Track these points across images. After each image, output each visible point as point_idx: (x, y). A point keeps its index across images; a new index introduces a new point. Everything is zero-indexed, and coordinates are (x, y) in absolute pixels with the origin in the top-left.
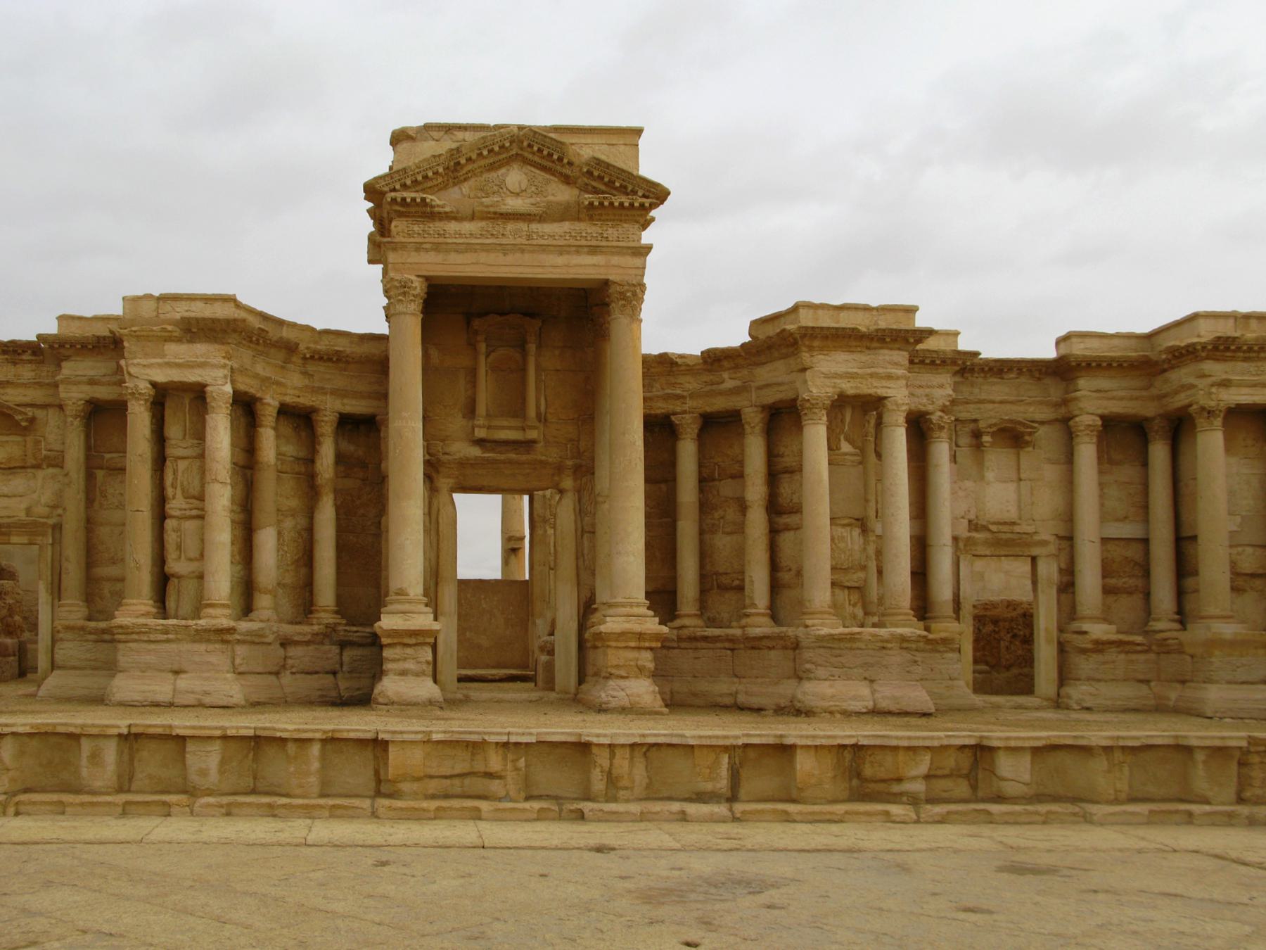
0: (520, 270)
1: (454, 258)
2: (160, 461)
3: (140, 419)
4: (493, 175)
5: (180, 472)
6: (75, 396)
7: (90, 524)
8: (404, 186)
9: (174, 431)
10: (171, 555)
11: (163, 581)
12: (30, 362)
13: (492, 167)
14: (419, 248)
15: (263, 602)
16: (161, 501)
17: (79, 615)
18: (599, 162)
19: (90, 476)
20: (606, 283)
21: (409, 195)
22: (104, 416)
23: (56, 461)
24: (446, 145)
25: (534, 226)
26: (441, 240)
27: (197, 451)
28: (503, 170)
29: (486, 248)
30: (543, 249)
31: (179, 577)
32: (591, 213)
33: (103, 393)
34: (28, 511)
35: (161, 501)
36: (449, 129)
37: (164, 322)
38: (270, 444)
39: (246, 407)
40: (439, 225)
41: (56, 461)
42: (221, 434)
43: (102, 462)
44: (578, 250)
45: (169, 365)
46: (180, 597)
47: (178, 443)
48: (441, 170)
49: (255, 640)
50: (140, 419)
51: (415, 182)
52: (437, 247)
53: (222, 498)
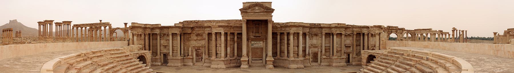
2: (216, 40)
3: (214, 36)
5: (218, 42)
6: (207, 32)
7: (209, 46)
9: (218, 37)
11: (217, 54)
15: (228, 56)
16: (216, 45)
19: (208, 41)
22: (210, 34)
23: (205, 39)
24: (249, 5)
33: (210, 32)
35: (216, 45)
38: (229, 38)
39: (226, 34)
41: (205, 39)
42: (223, 38)
43: (209, 40)
46: (219, 55)
47: (218, 39)
49: (227, 60)
50: (214, 36)
53: (223, 45)
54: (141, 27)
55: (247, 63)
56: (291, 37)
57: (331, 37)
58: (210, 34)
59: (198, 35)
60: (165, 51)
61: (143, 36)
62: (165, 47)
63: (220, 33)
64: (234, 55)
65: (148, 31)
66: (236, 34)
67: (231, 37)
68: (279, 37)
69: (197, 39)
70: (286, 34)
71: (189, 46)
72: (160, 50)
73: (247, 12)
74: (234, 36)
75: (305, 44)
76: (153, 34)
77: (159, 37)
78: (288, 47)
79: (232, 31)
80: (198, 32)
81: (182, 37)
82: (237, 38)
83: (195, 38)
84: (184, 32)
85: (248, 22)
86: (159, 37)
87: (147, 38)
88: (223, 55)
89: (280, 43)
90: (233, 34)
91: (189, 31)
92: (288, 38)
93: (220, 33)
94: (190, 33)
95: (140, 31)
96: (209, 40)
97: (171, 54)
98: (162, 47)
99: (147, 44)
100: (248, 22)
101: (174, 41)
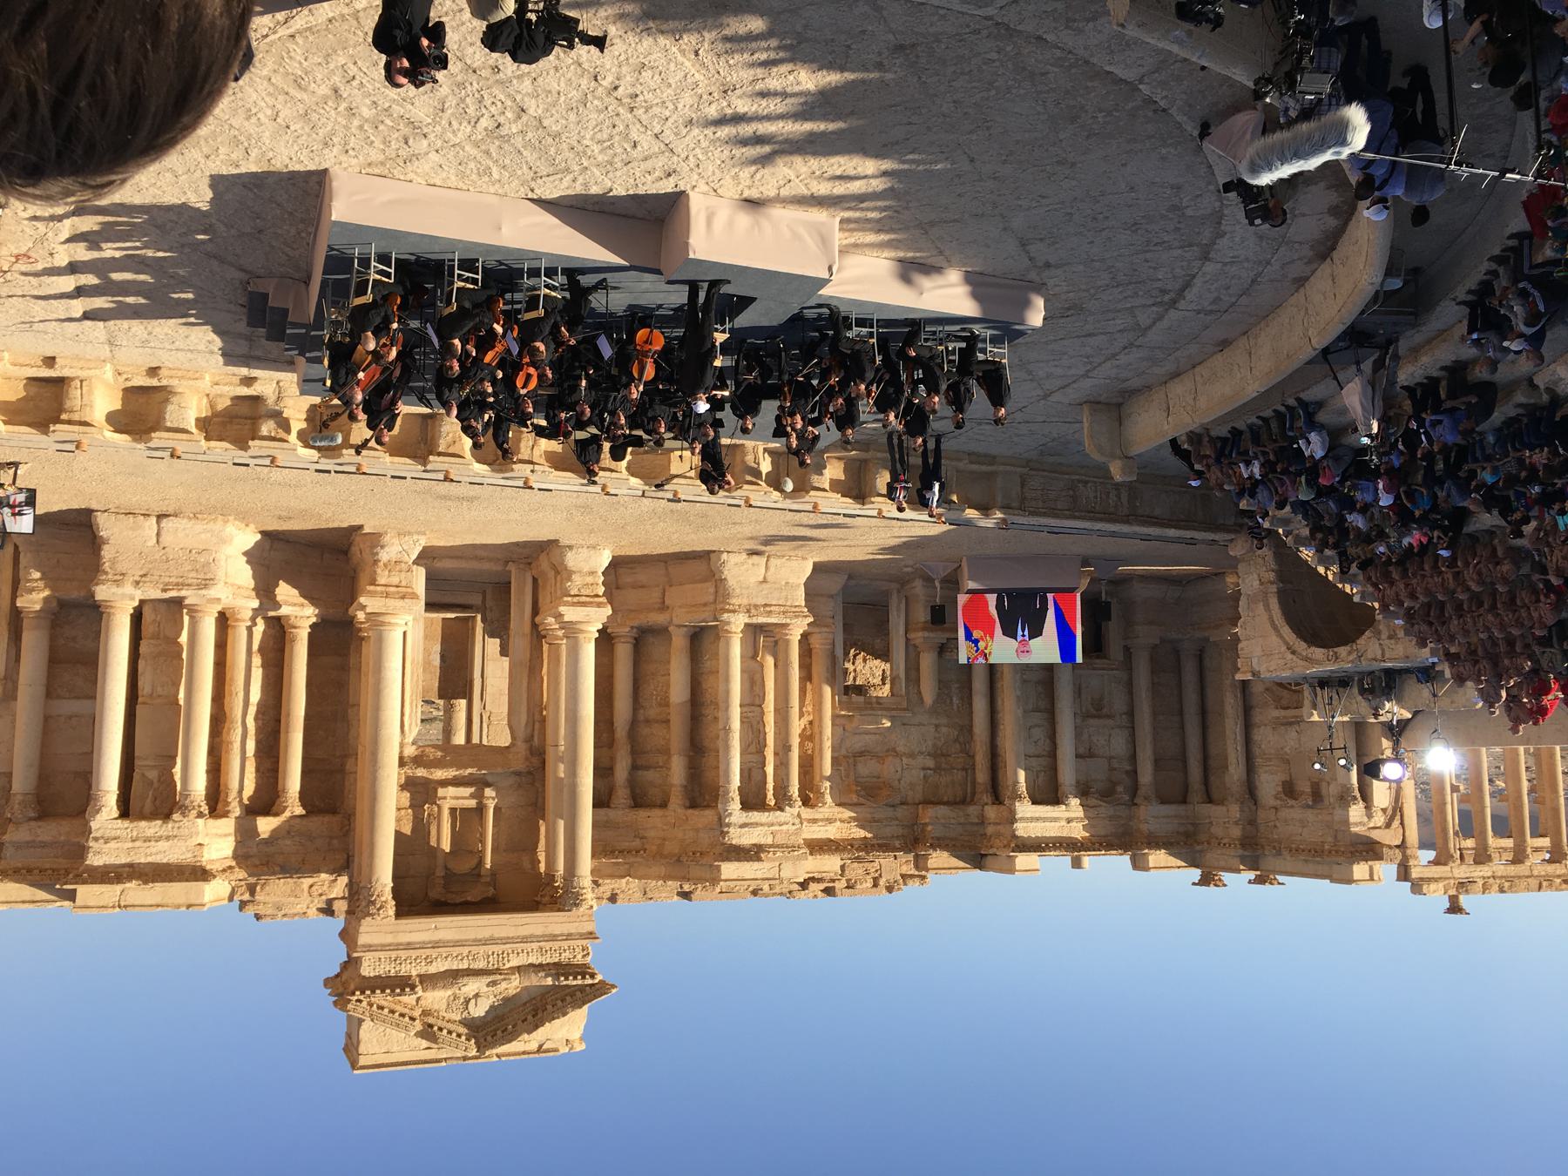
0: (480, 923)
1: (539, 930)
8: (581, 988)
20: (399, 914)
40: (547, 959)
48: (549, 1007)
52: (553, 938)
54: (1296, 851)
61: (1268, 784)
63: (746, 806)
65: (1225, 818)
67: (650, 775)
71: (934, 711)
72: (1130, 686)
73: (559, 969)
74: (632, 783)
75: (48, 725)
76: (1184, 801)
77: (1146, 775)
79: (651, 820)
81: (982, 776)
84: (973, 810)
86: (1146, 775)
87: (1235, 772)
90: (639, 801)
94: (927, 802)
95: (1297, 822)
98: (1119, 704)
99: (1232, 727)
100: (543, 894)
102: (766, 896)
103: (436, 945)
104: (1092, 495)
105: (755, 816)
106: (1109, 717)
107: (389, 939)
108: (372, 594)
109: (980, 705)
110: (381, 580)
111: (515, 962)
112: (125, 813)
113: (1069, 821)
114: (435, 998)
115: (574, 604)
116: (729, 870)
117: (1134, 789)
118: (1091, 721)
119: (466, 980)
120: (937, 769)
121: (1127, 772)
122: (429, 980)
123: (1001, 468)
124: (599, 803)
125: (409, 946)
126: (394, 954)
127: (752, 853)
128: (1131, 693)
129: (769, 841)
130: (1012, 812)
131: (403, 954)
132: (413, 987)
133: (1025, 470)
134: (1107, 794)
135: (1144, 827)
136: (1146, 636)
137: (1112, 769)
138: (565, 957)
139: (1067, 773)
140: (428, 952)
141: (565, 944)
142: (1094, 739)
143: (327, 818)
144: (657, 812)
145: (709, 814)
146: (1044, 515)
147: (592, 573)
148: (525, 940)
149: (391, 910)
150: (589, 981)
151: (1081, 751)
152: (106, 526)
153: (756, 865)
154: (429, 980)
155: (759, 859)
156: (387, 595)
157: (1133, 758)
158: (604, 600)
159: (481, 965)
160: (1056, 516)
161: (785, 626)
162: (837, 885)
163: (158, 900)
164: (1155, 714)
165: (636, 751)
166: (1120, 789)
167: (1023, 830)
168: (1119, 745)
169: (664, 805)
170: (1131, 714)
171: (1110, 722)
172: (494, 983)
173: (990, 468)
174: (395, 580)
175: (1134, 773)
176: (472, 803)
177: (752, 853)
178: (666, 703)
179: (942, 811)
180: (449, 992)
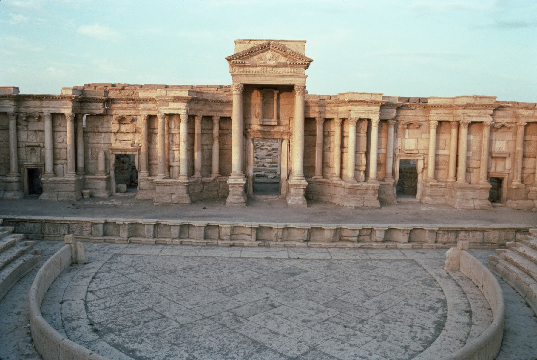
1: (251, 78)
4: (262, 54)
8: (237, 58)
10: (171, 160)
12: (131, 103)
13: (262, 52)
14: (241, 75)
17: (146, 175)
18: (293, 52)
21: (238, 61)
22: (151, 118)
24: (250, 46)
25: (274, 69)
26: (247, 73)
27: (178, 132)
28: (266, 53)
29: (261, 76)
30: (276, 76)
31: (173, 167)
32: (292, 65)
33: (152, 113)
34: (132, 145)
36: (250, 41)
37: (168, 97)
39: (191, 118)
44: (287, 76)
45: (170, 109)
51: (240, 57)
55: (241, 190)
56: (350, 130)
57: (454, 131)
58: (151, 118)
59: (121, 120)
60: (33, 160)
62: (33, 148)
64: (210, 172)
66: (216, 121)
68: (319, 129)
69: (119, 132)
70: (337, 121)
73: (244, 66)
74: (213, 125)
77: (12, 124)
78: (342, 153)
80: (121, 113)
82: (220, 128)
83: (115, 127)
85: (247, 90)
88: (183, 170)
89: (324, 144)
91: (99, 108)
92: (342, 132)
93: (178, 115)
96: (151, 133)
97: (49, 167)
98: (23, 151)
100: (247, 90)
101: (58, 135)
102: (137, 85)
103: (283, 76)
104: (62, 230)
105: (175, 112)
106: (29, 146)
107: (298, 79)
108: (304, 186)
109: (80, 151)
110: (302, 190)
111: (258, 69)
112: (369, 120)
113: (48, 107)
114: (282, 60)
115: (239, 184)
116: (185, 94)
117: (17, 118)
118: (36, 144)
119: (274, 65)
120: (98, 127)
121: (20, 125)
122: (285, 65)
123: (102, 238)
124: (229, 119)
125: (291, 76)
126: (296, 74)
127: (177, 99)
128: (18, 156)
129: (170, 104)
130: (73, 111)
131: (292, 74)
132: (290, 64)
133: (91, 238)
134: (29, 117)
135: (12, 103)
136: (13, 178)
137: (27, 126)
138: (241, 69)
139: (47, 124)
140: (285, 74)
141: (241, 73)
142: (34, 138)
143: (327, 117)
144: (205, 114)
145: (191, 114)
146: (82, 221)
147: (234, 195)
148: (255, 76)
149: (296, 88)
150: (235, 61)
151: (40, 133)
152: (377, 203)
153: (175, 95)
154: (285, 65)
155: (174, 97)
156: (300, 185)
157: (18, 130)
158: (230, 186)
159: (269, 69)
160: (78, 221)
161: (164, 178)
162: (111, 88)
163: (362, 95)
164: (8, 147)
165: (212, 134)
166: (24, 118)
167: (70, 104)
168: (23, 136)
169: (204, 117)
170: (18, 147)
171: (28, 144)
172: (265, 63)
173: (105, 238)
174: (297, 190)
175: (18, 124)
176: (265, 120)
177: (177, 99)
178: (203, 150)
179: (98, 112)
180: (279, 61)
